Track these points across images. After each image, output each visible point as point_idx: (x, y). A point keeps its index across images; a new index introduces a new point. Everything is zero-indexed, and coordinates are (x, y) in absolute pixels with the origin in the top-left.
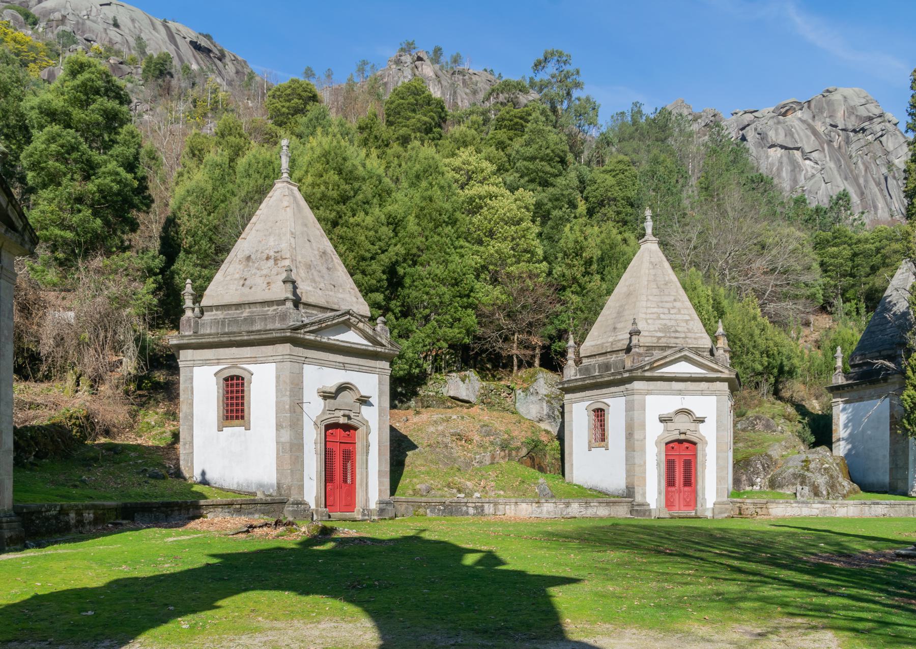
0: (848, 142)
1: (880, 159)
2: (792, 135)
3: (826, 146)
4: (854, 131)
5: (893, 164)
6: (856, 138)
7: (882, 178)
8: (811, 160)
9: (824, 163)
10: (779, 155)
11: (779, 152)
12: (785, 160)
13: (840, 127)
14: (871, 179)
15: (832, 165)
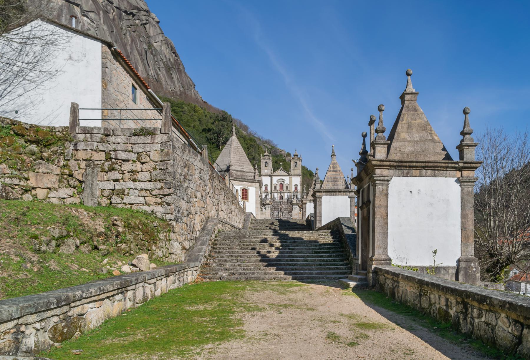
0: (120, 18)
1: (143, 38)
3: (101, 12)
5: (152, 45)
6: (127, 18)
7: (143, 50)
13: (115, 5)
14: (135, 48)
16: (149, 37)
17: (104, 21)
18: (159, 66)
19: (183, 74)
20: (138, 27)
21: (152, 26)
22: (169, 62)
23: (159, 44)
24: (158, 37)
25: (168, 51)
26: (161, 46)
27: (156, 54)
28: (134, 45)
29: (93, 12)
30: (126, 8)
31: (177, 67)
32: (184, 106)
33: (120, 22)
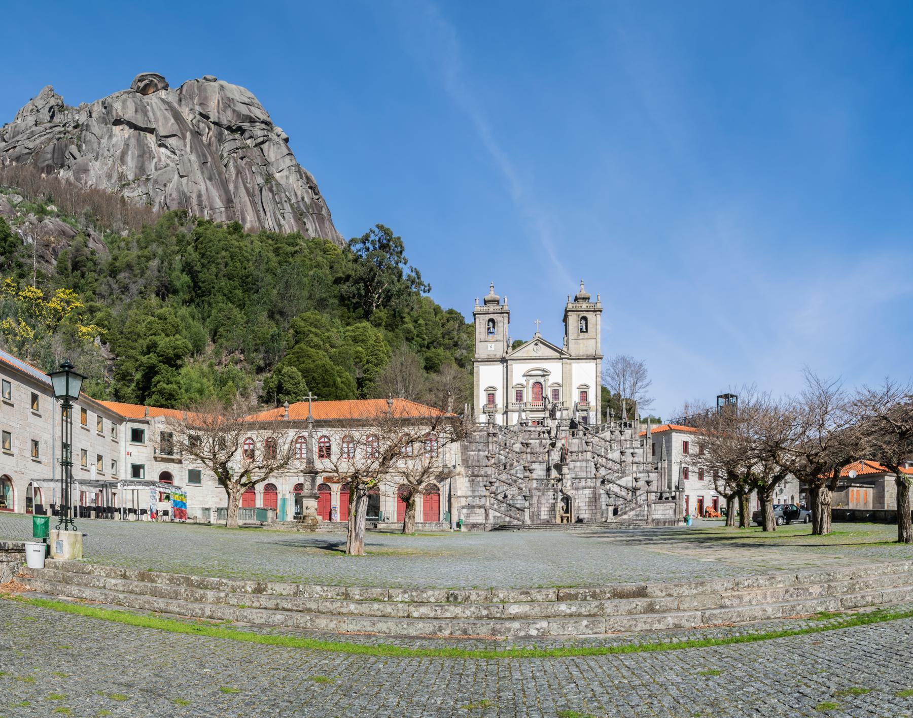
0: (220, 139)
2: (145, 113)
3: (188, 135)
4: (229, 128)
6: (231, 137)
7: (257, 187)
8: (167, 147)
9: (183, 153)
10: (126, 136)
11: (127, 132)
12: (133, 142)
13: (212, 119)
15: (193, 158)
16: (267, 164)
17: (191, 147)
18: (282, 211)
19: (327, 224)
20: (249, 150)
22: (301, 204)
23: (285, 173)
24: (284, 162)
25: (300, 184)
26: (287, 177)
27: (278, 190)
28: (240, 180)
29: (174, 135)
31: (316, 212)
32: (298, 241)
33: (220, 145)
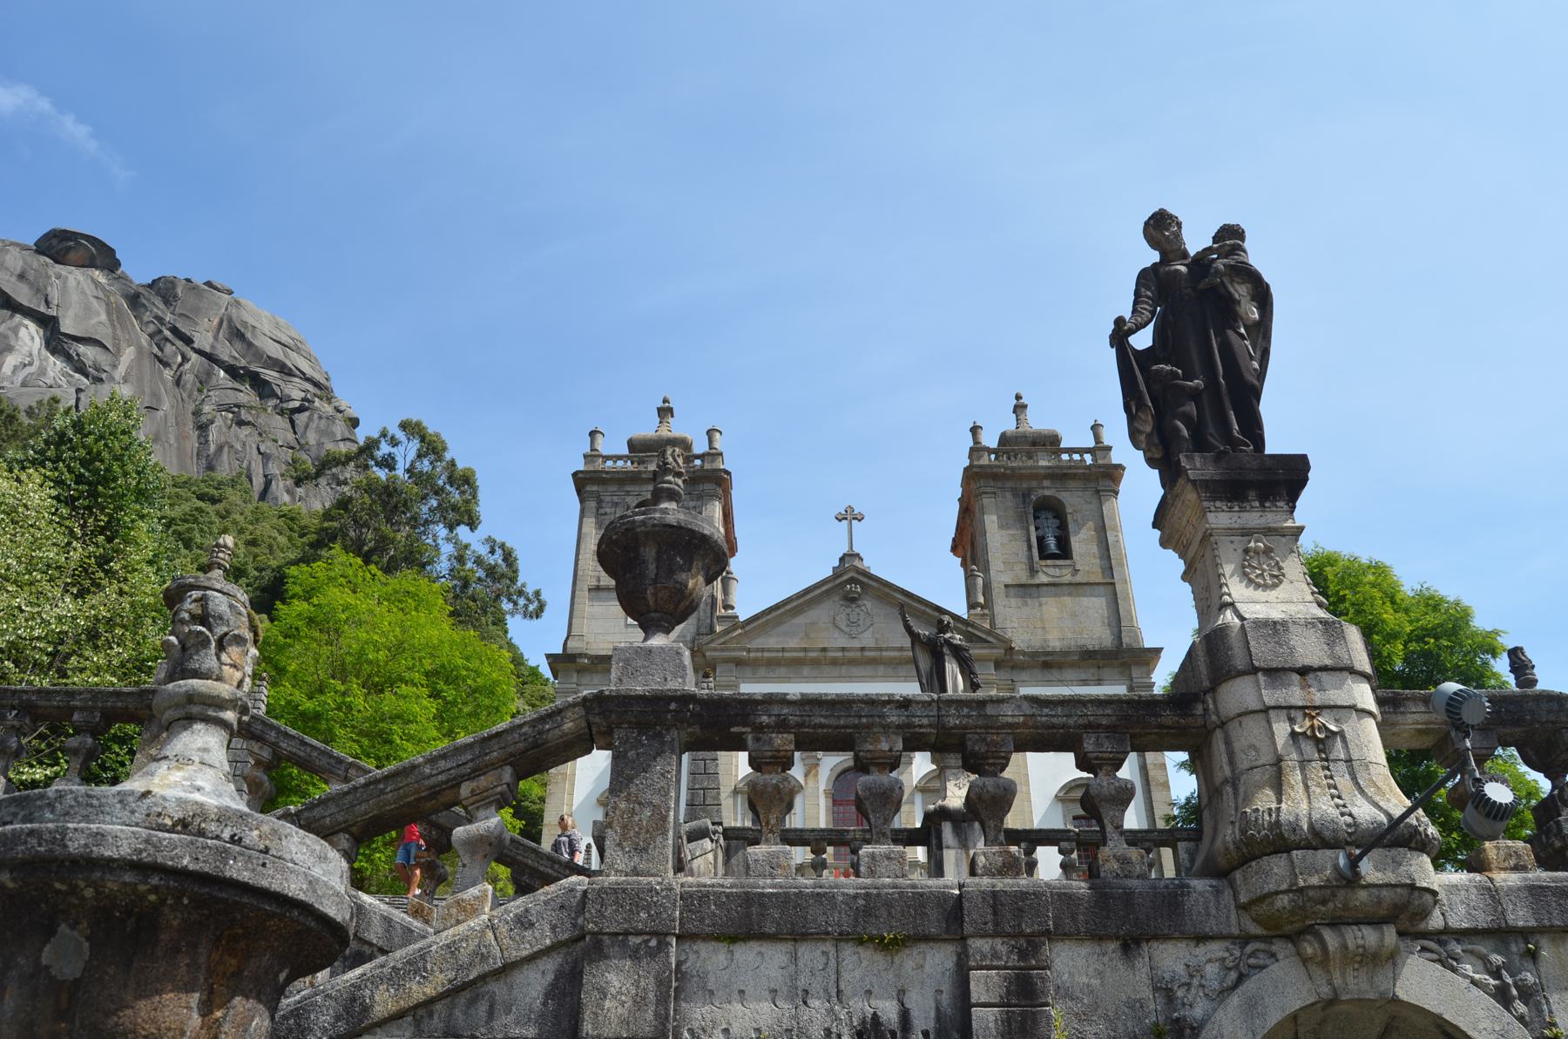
6: (230, 384)
21: (320, 417)
30: (235, 358)
